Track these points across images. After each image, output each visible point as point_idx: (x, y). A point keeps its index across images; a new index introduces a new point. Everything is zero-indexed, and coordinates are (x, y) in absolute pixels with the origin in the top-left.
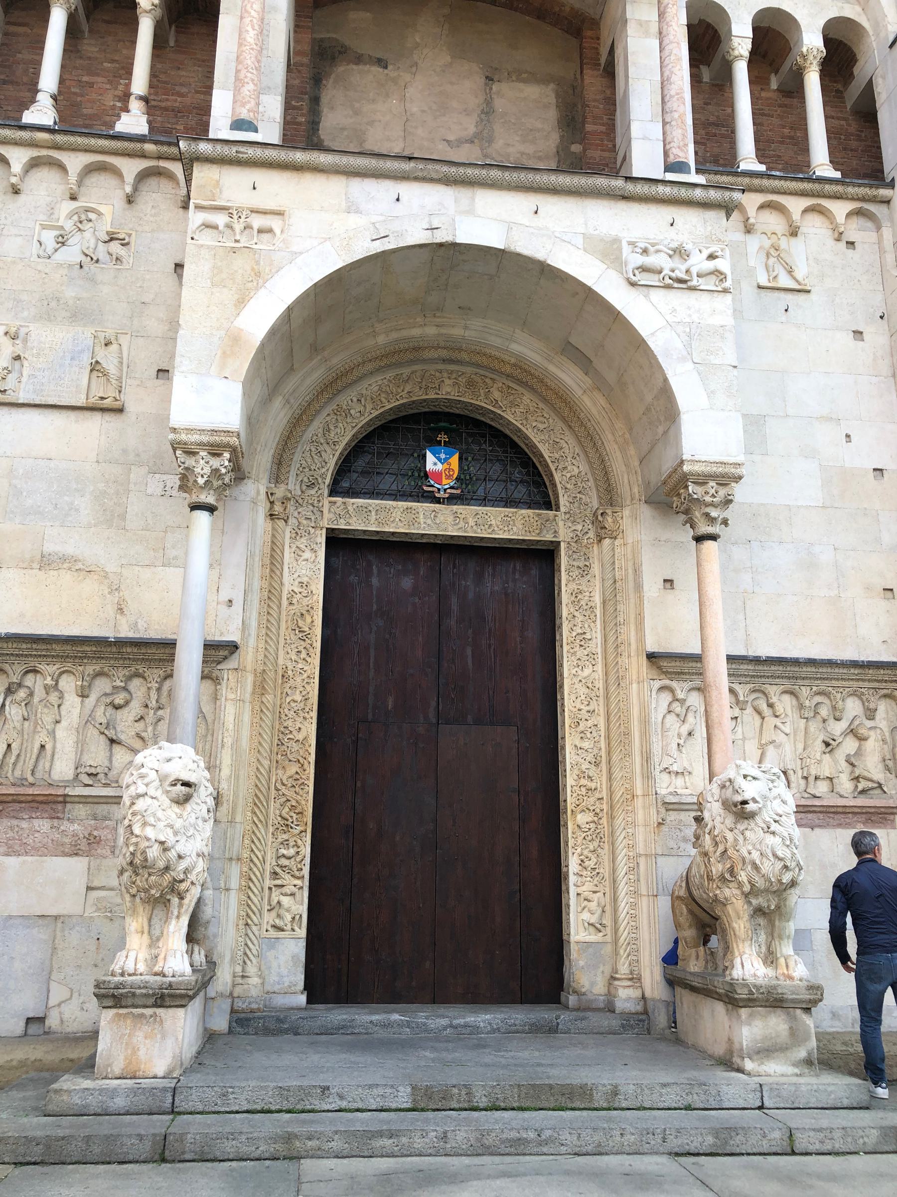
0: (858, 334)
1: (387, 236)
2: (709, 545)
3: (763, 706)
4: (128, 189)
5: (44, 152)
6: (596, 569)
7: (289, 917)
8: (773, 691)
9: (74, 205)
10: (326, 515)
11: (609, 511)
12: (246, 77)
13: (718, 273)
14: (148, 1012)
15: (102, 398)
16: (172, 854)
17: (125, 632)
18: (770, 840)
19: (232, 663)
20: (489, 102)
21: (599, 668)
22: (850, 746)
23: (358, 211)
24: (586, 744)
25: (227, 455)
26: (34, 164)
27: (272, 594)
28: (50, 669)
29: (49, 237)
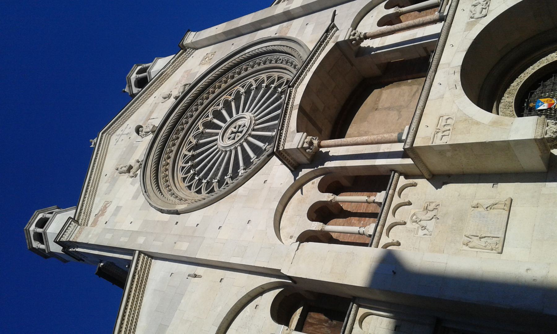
1: (455, 85)
12: (381, 136)
20: (385, 109)
23: (443, 95)
29: (421, 233)
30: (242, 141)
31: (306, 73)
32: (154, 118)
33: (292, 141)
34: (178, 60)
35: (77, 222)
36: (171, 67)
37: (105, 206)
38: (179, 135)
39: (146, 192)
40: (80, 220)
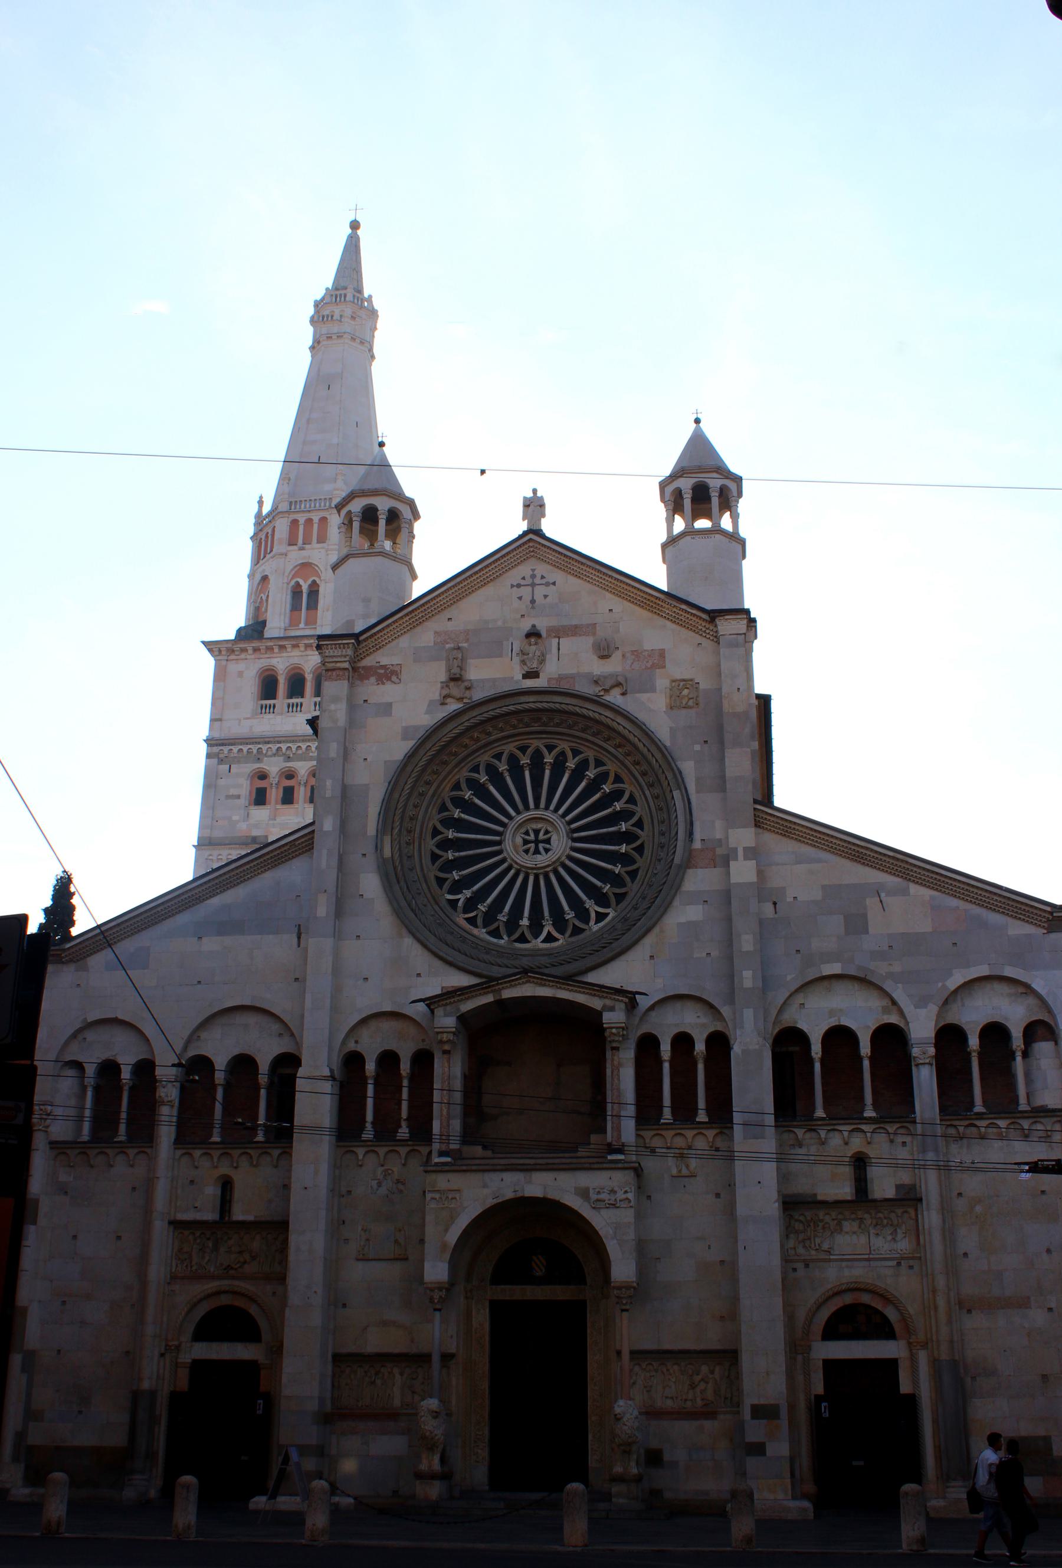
0: (718, 1195)
2: (625, 1314)
3: (665, 1370)
4: (403, 1162)
9: (383, 1168)
13: (627, 1199)
15: (400, 1255)
18: (625, 1428)
22: (702, 1385)
25: (444, 1291)
26: (367, 1152)
29: (374, 1183)
30: (515, 866)
31: (553, 986)
32: (559, 649)
34: (690, 617)
35: (359, 642)
36: (675, 610)
40: (365, 644)
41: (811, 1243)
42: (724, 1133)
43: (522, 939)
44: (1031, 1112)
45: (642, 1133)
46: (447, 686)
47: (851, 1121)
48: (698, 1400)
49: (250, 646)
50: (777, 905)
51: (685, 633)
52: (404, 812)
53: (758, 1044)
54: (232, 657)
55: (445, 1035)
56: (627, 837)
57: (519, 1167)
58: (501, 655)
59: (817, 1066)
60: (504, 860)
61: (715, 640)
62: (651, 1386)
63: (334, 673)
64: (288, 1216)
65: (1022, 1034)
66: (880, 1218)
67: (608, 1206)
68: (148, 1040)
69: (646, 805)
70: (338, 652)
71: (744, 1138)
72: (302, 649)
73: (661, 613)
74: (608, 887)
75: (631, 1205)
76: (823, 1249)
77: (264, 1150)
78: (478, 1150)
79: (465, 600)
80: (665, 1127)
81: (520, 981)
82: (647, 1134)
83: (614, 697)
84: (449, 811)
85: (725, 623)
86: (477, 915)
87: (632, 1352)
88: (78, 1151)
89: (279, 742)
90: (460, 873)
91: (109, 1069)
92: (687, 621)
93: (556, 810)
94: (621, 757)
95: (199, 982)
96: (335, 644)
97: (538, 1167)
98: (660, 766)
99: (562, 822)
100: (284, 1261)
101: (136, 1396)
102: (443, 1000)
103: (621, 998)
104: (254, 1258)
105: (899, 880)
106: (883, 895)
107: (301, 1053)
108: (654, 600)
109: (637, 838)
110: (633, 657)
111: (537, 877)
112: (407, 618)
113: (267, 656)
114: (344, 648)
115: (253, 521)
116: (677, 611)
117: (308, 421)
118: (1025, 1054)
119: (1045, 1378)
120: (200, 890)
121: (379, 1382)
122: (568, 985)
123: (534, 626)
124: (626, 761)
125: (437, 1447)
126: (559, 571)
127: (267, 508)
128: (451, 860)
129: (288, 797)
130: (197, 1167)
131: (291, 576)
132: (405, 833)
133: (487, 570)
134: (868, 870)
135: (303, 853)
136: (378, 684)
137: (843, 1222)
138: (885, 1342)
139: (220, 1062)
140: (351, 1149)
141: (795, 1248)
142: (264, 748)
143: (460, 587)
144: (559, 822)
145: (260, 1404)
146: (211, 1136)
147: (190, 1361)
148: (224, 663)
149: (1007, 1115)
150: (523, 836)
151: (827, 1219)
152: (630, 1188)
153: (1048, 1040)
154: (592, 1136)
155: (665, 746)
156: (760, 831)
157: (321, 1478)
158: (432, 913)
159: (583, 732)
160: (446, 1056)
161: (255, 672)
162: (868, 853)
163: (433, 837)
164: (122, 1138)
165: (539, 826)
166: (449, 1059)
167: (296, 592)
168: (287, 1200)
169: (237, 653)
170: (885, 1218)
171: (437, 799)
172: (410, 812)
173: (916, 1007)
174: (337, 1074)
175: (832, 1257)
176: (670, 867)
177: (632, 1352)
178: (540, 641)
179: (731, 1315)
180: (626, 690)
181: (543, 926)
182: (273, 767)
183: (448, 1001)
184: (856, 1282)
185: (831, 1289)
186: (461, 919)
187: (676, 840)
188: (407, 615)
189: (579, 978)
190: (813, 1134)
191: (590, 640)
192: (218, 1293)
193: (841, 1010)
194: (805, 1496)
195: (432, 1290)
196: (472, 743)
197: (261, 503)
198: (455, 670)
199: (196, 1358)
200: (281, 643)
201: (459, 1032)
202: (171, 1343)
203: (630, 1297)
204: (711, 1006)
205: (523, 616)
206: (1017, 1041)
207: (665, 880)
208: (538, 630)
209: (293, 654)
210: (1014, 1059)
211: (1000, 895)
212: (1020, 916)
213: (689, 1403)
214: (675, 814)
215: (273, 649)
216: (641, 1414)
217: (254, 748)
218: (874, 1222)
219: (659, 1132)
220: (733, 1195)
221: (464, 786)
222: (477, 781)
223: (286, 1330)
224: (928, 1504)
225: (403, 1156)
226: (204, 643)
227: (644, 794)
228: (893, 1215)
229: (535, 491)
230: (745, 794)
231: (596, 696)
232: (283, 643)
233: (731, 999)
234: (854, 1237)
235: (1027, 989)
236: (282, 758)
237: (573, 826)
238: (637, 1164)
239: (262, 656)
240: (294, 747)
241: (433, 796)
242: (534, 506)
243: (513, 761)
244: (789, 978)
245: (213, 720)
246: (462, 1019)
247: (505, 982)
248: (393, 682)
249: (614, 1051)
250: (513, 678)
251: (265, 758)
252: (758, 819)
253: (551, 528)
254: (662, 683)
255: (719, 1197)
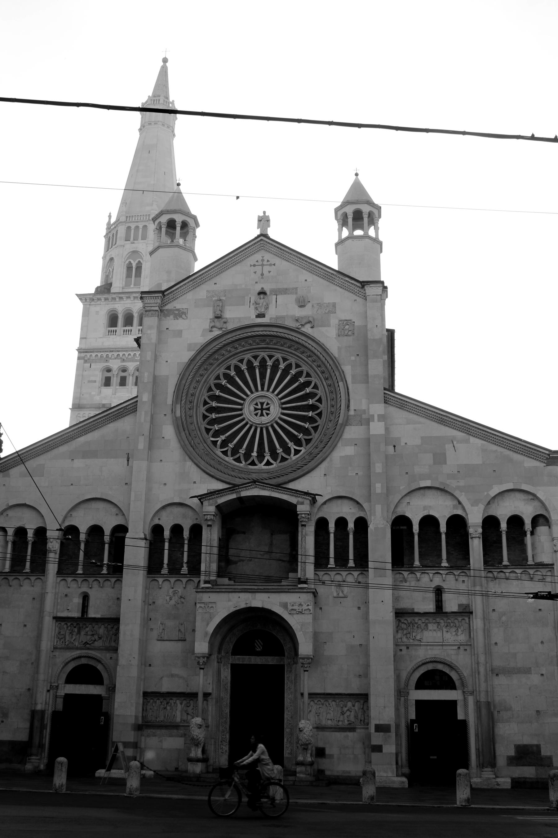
0: (359, 608)
2: (306, 672)
4: (184, 586)
5: (166, 578)
6: (293, 671)
7: (224, 751)
8: (330, 701)
9: (173, 590)
10: (230, 660)
11: (295, 658)
13: (308, 609)
14: (196, 763)
15: (181, 638)
16: (198, 737)
17: (188, 691)
18: (305, 735)
19: (210, 697)
21: (293, 695)
22: (348, 713)
23: (231, 601)
24: (289, 713)
25: (206, 658)
26: (164, 581)
27: (219, 680)
28: (175, 699)
29: (168, 598)
32: (276, 302)
33: (209, 505)
34: (350, 285)
35: (164, 296)
36: (342, 280)
37: (184, 313)
38: (261, 343)
39: (192, 360)
40: (167, 296)
41: (410, 636)
42: (363, 573)
43: (253, 463)
44: (534, 565)
45: (317, 573)
46: (213, 321)
47: (434, 568)
48: (346, 721)
49: (103, 297)
50: (396, 447)
51: (347, 293)
52: (188, 391)
53: (383, 524)
54: (93, 303)
55: (209, 516)
56: (313, 408)
57: (249, 590)
58: (244, 305)
59: (416, 538)
60: (243, 419)
61: (364, 298)
62: (320, 713)
63: (150, 313)
64: (120, 615)
65: (530, 522)
66: (449, 622)
67: (298, 613)
68: (43, 516)
69: (324, 390)
70: (152, 301)
71: (375, 577)
72: (132, 299)
73: (334, 283)
74: (301, 435)
75: (311, 612)
76: (417, 639)
77: (106, 579)
78: (226, 581)
79: (224, 273)
80: (330, 569)
81: (251, 487)
82: (321, 573)
83: (307, 329)
84: (213, 391)
85: (370, 289)
86: (228, 450)
87: (310, 694)
88: (3, 577)
89: (119, 351)
90: (219, 426)
91: (21, 532)
92: (348, 287)
93: (273, 392)
94: (310, 363)
95: (72, 484)
96: (151, 297)
97: (259, 590)
98: (332, 368)
99: (277, 399)
100: (117, 640)
101: (33, 713)
102: (208, 497)
103: (307, 497)
104: (100, 638)
105: (465, 434)
106: (455, 443)
107: (128, 524)
108: (330, 275)
109: (318, 408)
110: (318, 307)
111: (261, 429)
112: (191, 283)
113: (113, 303)
114: (156, 299)
115: (106, 227)
116: (343, 281)
117: (137, 171)
118: (532, 533)
119: (538, 711)
120: (73, 433)
121: (168, 708)
122: (278, 489)
123: (262, 288)
124: (313, 365)
125: (200, 745)
126: (278, 258)
127: (113, 220)
128: (214, 419)
129: (123, 382)
130: (69, 587)
131: (126, 258)
132: (188, 403)
133: (237, 256)
134: (447, 428)
135: (131, 413)
136: (175, 319)
137: (428, 624)
138: (450, 691)
139: (83, 529)
140: (156, 579)
141: (401, 638)
142: (110, 354)
143: (221, 266)
144: (274, 398)
145: (102, 719)
146: (77, 570)
147: (64, 694)
148: (88, 306)
149: (521, 567)
150: (254, 406)
151: (420, 622)
152: (311, 603)
153: (545, 526)
154: (289, 574)
155: (335, 357)
156: (388, 405)
157: (135, 760)
158: (203, 448)
159: (288, 348)
160: (209, 528)
161: (105, 311)
162: (447, 419)
163: (204, 405)
164: (28, 571)
165: (263, 400)
166: (211, 529)
167: (129, 268)
168: (119, 606)
169: (95, 301)
170: (452, 623)
171: (206, 385)
172: (191, 392)
173: (472, 505)
174: (148, 537)
175: (422, 643)
176: (337, 425)
177: (310, 694)
178: (265, 297)
179: (365, 675)
180: (314, 325)
181: (265, 457)
182: (115, 365)
183: (211, 497)
184: (435, 658)
185: (421, 661)
186: (218, 451)
187: (340, 410)
188: (191, 281)
189: (284, 486)
190: (413, 575)
191: (294, 297)
192: (80, 657)
193: (430, 506)
194: (403, 775)
195: (199, 658)
196: (227, 353)
197: (110, 217)
198: (218, 312)
199: (67, 693)
200: (120, 296)
201: (217, 515)
202: (53, 685)
203: (309, 663)
204: (358, 503)
205: (257, 282)
206: (528, 526)
207: (333, 432)
208: (264, 290)
209: (126, 302)
210: (526, 536)
211: (520, 444)
212: (532, 456)
213: (340, 723)
214: (340, 395)
215: (116, 299)
216: (314, 728)
217: (104, 354)
218: (446, 625)
219: (327, 572)
220: (368, 608)
221: (222, 377)
222: (229, 375)
223: (118, 679)
224: (472, 781)
225: (184, 583)
226: (77, 295)
227: (323, 384)
228: (456, 621)
229: (264, 212)
230: (380, 384)
231: (297, 328)
232: (121, 295)
233: (369, 498)
234: (435, 632)
235: (534, 497)
236: (119, 360)
237: (283, 401)
238: (315, 590)
239: (109, 303)
240: (127, 354)
241: (204, 382)
242: (264, 221)
243: (249, 363)
244: (401, 488)
245: (81, 338)
246: (218, 507)
247: (243, 487)
248: (183, 318)
249: (303, 527)
250: (250, 317)
251: (111, 360)
252: (386, 399)
253: (272, 233)
254: (334, 321)
255: (360, 609)
